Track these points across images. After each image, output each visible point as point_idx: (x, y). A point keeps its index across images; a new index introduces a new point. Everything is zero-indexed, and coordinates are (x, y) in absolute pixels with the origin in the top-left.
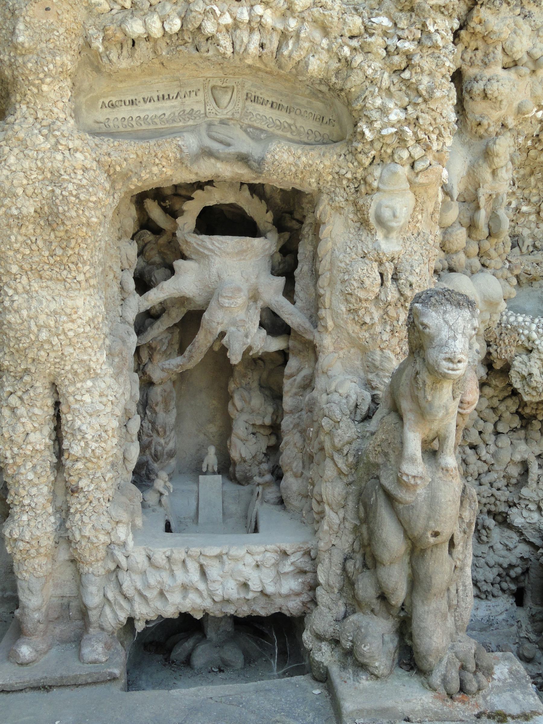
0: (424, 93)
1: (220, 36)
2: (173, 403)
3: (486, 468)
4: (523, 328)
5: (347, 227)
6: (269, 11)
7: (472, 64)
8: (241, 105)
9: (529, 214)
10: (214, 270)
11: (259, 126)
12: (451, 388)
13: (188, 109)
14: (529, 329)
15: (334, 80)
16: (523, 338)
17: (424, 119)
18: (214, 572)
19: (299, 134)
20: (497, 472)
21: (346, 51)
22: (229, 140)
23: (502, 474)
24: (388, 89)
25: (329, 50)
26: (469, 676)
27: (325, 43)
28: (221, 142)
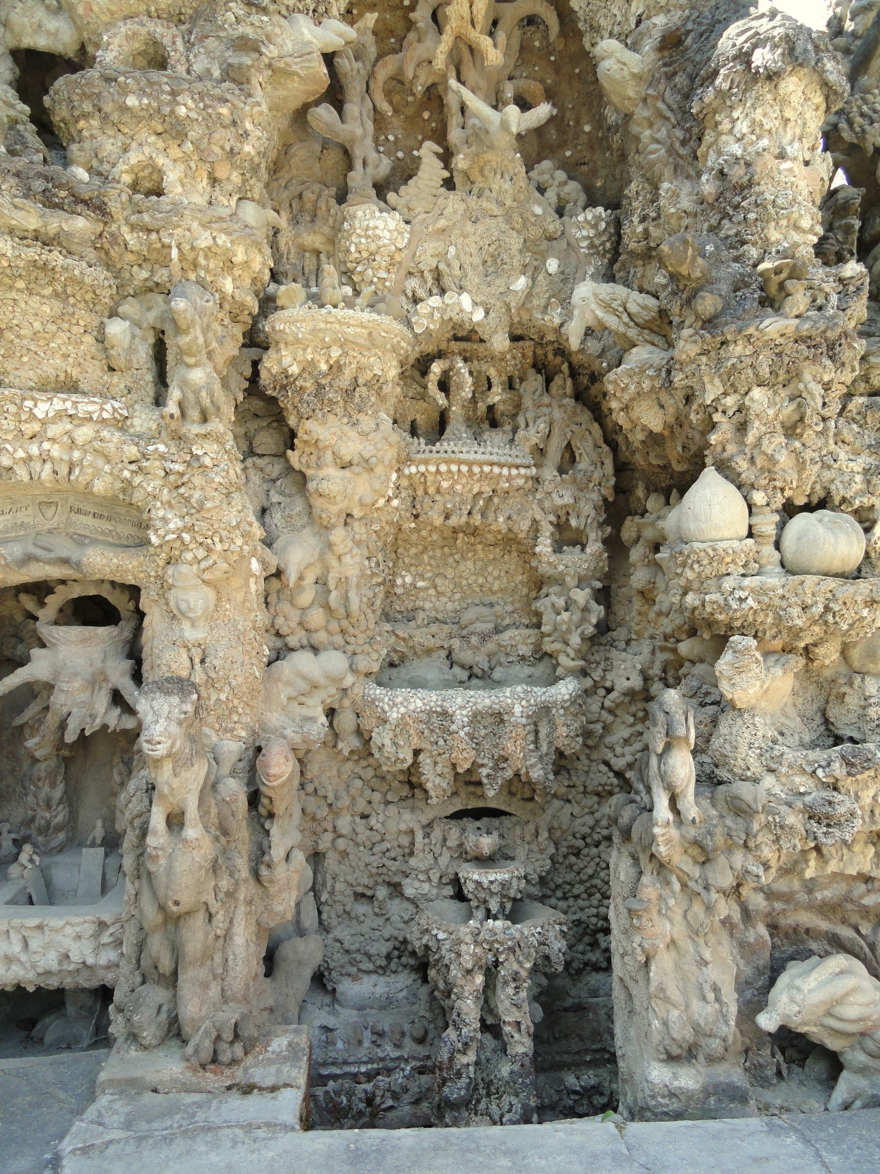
0: (195, 505)
1: (16, 467)
2: (60, 778)
3: (379, 838)
4: (379, 700)
5: (163, 617)
6: (56, 446)
7: (308, 467)
8: (65, 516)
9: (427, 589)
10: (61, 657)
11: (82, 533)
12: (171, 766)
13: (19, 522)
14: (383, 701)
15: (121, 496)
16: (379, 710)
17: (200, 526)
18: (34, 944)
19: (120, 538)
20: (389, 841)
21: (126, 474)
22: (49, 546)
23: (396, 844)
24: (169, 502)
25: (111, 474)
26: (223, 1046)
27: (107, 468)
28: (45, 549)
